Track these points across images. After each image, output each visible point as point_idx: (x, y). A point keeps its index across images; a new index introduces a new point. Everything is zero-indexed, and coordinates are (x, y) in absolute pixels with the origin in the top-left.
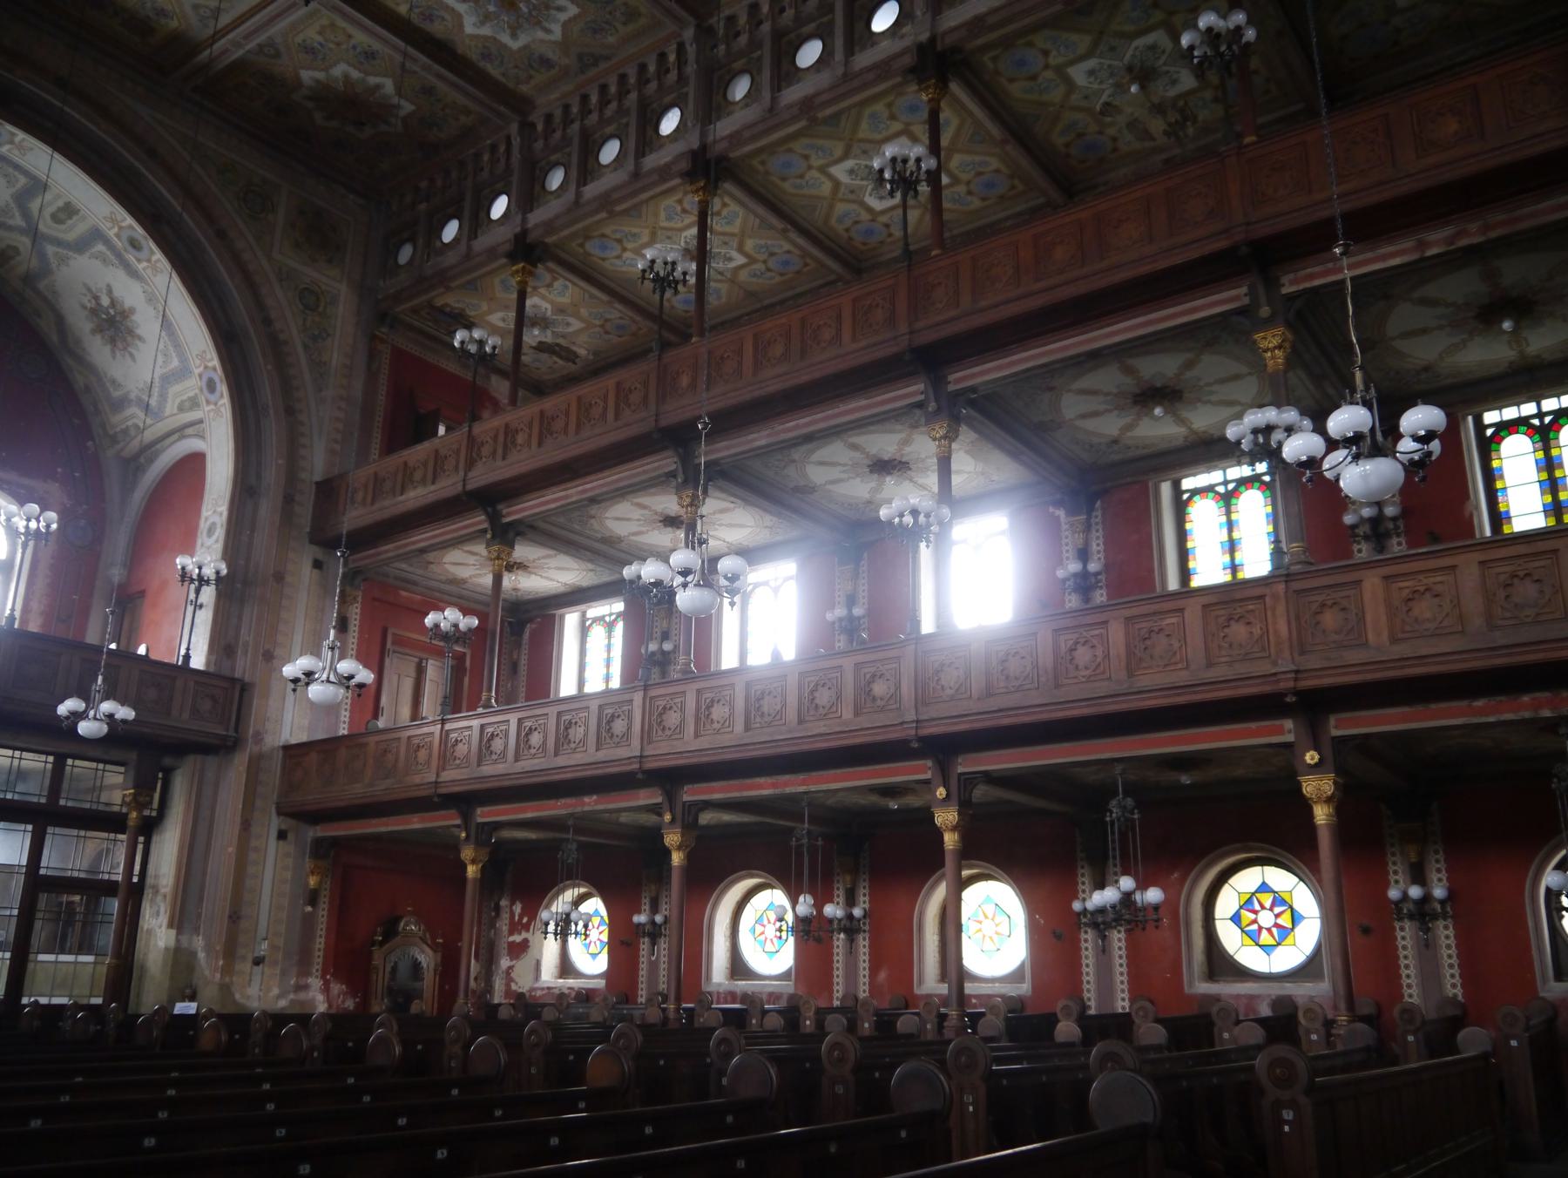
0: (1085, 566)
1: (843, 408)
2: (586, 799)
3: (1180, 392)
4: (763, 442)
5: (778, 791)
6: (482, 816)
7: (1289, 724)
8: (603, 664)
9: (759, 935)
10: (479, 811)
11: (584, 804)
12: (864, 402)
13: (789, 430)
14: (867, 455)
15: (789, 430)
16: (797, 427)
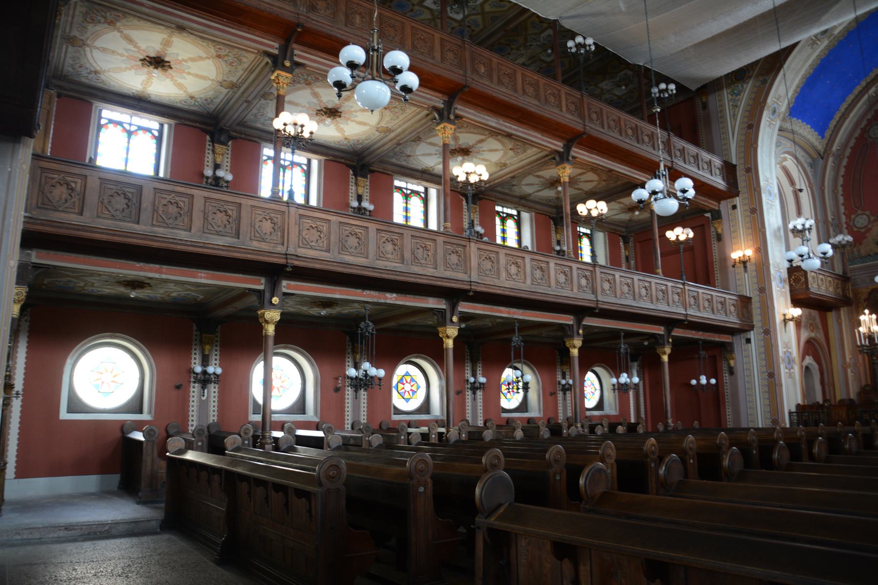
0: (360, 204)
1: (532, 133)
2: (388, 295)
3: (317, 114)
4: (494, 125)
5: (510, 316)
6: (288, 287)
7: (663, 328)
8: (125, 152)
9: (283, 382)
10: (284, 283)
11: (386, 298)
12: (539, 136)
13: (507, 127)
14: (321, 102)
15: (507, 127)
16: (510, 128)
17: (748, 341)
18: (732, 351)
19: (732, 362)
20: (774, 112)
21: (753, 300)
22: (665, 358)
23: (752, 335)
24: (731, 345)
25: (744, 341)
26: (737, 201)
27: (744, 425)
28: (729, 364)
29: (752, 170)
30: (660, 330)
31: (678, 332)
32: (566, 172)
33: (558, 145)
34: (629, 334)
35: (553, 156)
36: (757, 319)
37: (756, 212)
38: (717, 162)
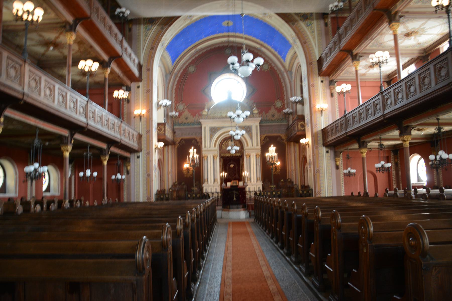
17: (138, 157)
18: (129, 162)
19: (129, 168)
20: (163, 45)
21: (143, 136)
22: (105, 163)
23: (140, 154)
24: (129, 158)
25: (136, 157)
26: (141, 84)
27: (133, 200)
28: (127, 169)
29: (150, 70)
30: (104, 146)
31: (113, 149)
32: (70, 39)
33: (70, 19)
34: (93, 147)
35: (64, 24)
36: (144, 147)
37: (149, 91)
38: (137, 61)
